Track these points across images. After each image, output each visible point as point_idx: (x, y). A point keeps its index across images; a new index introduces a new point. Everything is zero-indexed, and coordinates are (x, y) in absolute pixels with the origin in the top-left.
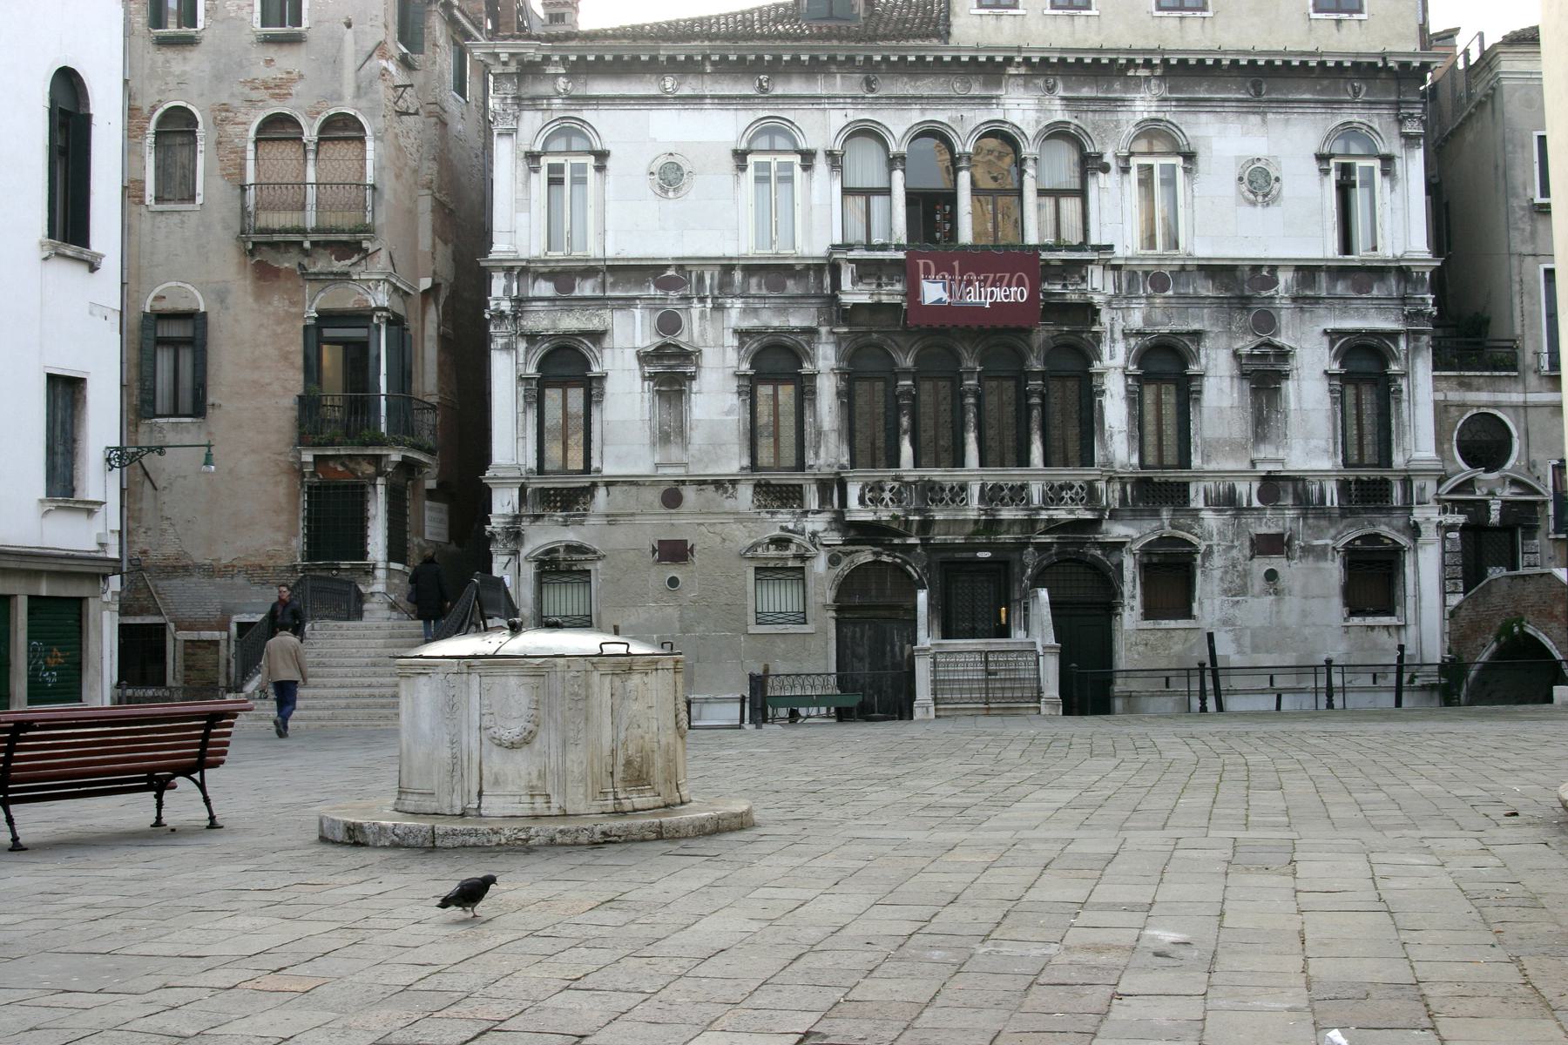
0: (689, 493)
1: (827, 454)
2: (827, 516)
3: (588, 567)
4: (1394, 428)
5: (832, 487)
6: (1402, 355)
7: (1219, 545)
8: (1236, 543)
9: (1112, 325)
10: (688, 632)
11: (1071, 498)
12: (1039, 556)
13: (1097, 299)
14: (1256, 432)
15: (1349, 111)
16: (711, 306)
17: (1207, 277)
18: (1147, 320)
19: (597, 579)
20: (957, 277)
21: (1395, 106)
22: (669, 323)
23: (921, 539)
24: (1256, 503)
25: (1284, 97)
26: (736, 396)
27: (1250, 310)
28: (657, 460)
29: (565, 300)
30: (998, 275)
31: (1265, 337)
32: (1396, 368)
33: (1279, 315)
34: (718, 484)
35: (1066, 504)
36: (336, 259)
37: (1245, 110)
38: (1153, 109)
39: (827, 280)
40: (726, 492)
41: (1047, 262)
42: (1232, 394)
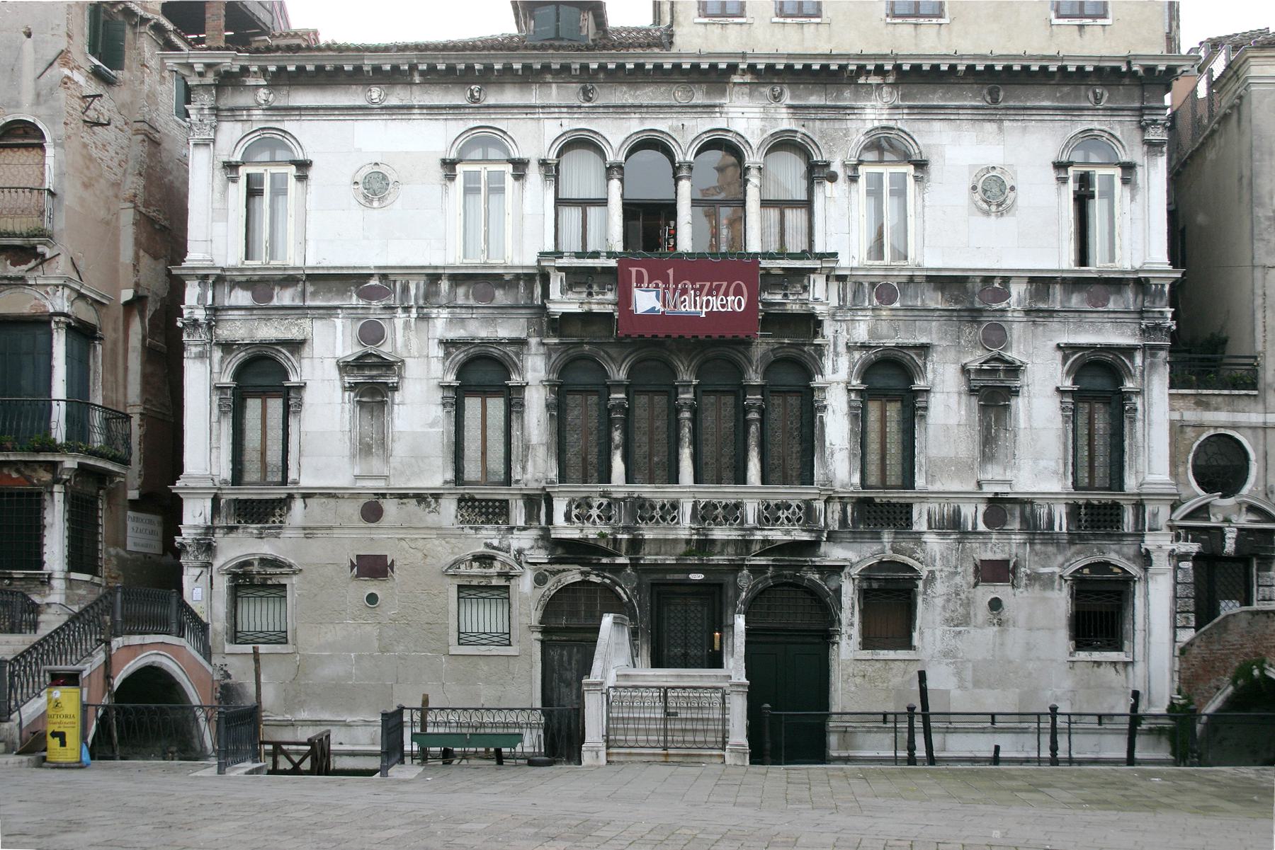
0: (389, 506)
1: (535, 468)
2: (534, 533)
3: (283, 581)
4: (1127, 449)
5: (538, 502)
6: (1138, 373)
7: (942, 570)
8: (959, 570)
9: (835, 338)
10: (388, 651)
11: (787, 518)
13: (819, 309)
14: (984, 452)
15: (1090, 118)
16: (415, 316)
17: (935, 289)
18: (872, 333)
19: (293, 594)
20: (672, 286)
21: (1137, 113)
22: (371, 333)
23: (630, 559)
24: (981, 527)
25: (1021, 104)
26: (441, 408)
27: (980, 323)
28: (357, 472)
29: (263, 308)
30: (715, 284)
31: (996, 351)
32: (1131, 385)
33: (1011, 329)
34: (420, 498)
35: (782, 524)
36: (12, 264)
37: (980, 117)
38: (885, 117)
39: (538, 290)
40: (429, 506)
41: (768, 272)
42: (959, 412)
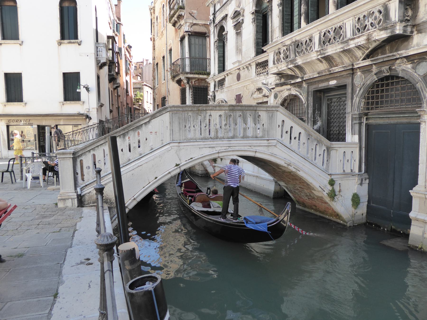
12: (365, 78)
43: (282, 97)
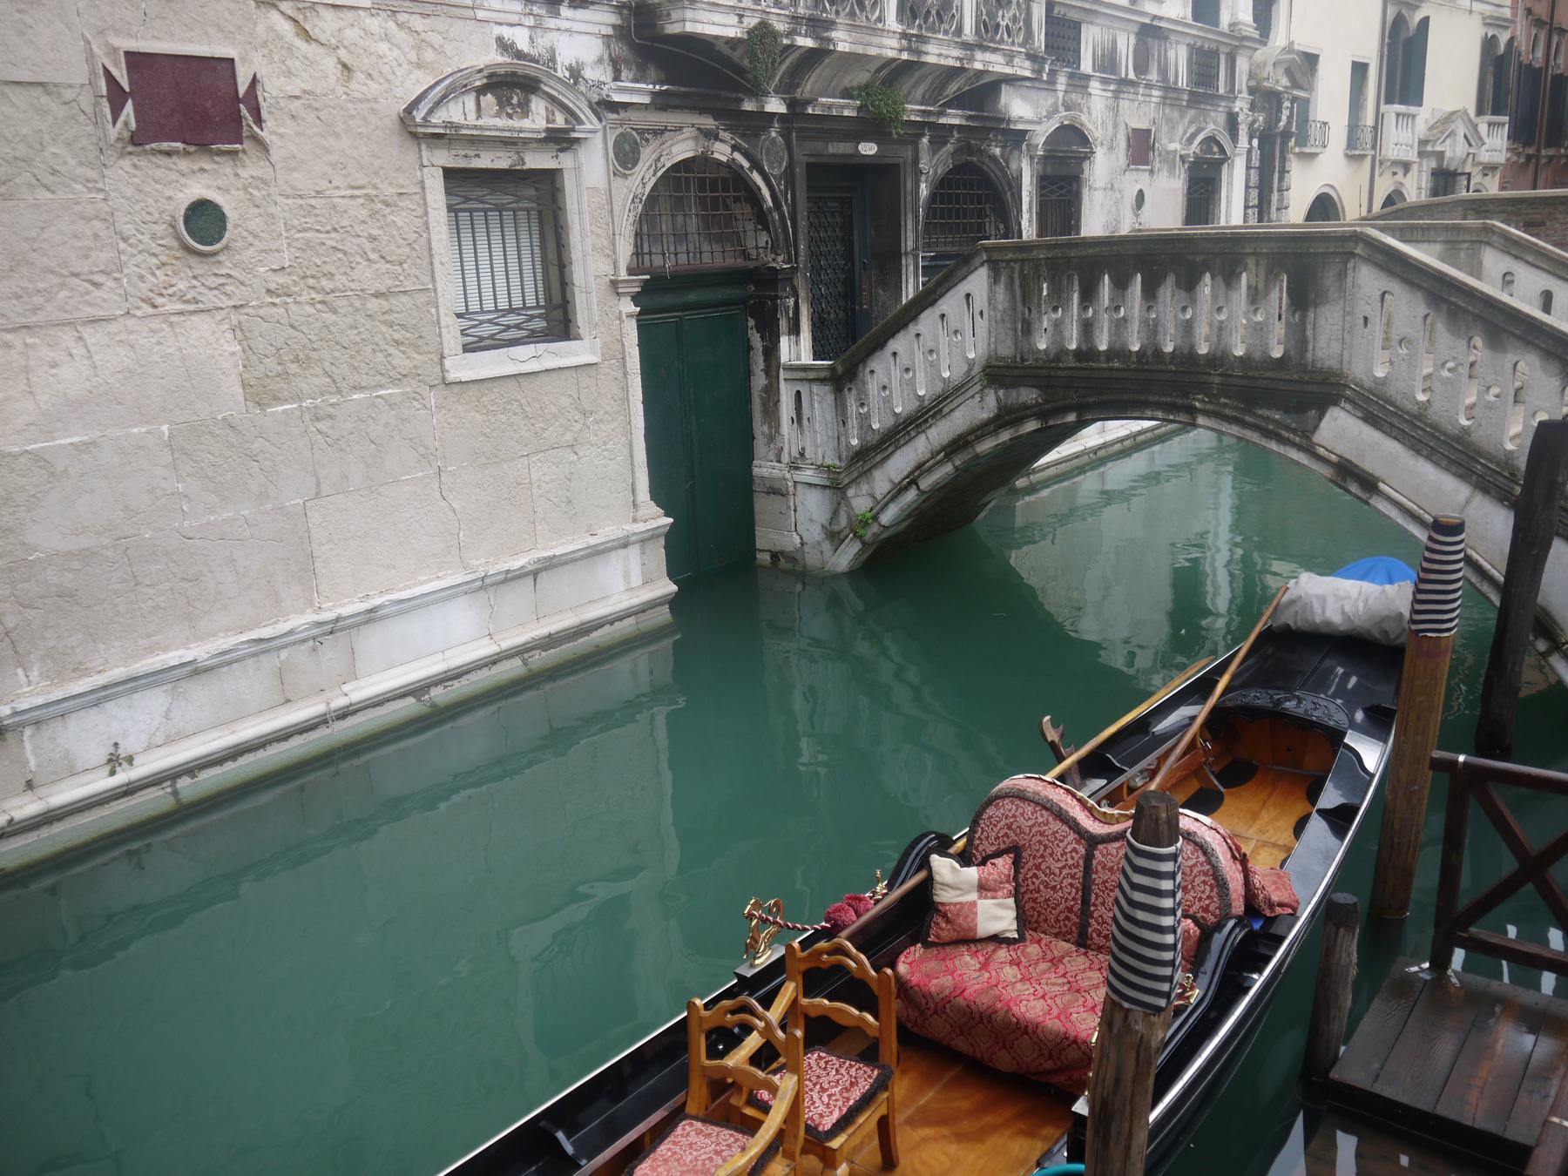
10: (277, 399)
23: (792, 104)
24: (1132, 76)
35: (1002, 40)
43: (659, 165)
